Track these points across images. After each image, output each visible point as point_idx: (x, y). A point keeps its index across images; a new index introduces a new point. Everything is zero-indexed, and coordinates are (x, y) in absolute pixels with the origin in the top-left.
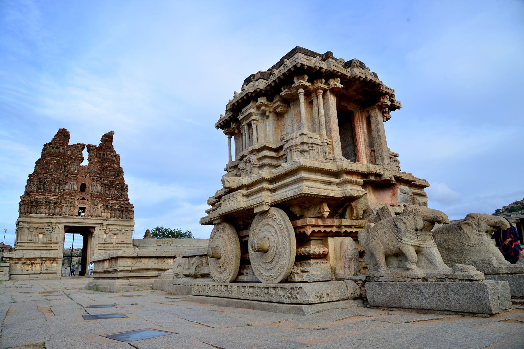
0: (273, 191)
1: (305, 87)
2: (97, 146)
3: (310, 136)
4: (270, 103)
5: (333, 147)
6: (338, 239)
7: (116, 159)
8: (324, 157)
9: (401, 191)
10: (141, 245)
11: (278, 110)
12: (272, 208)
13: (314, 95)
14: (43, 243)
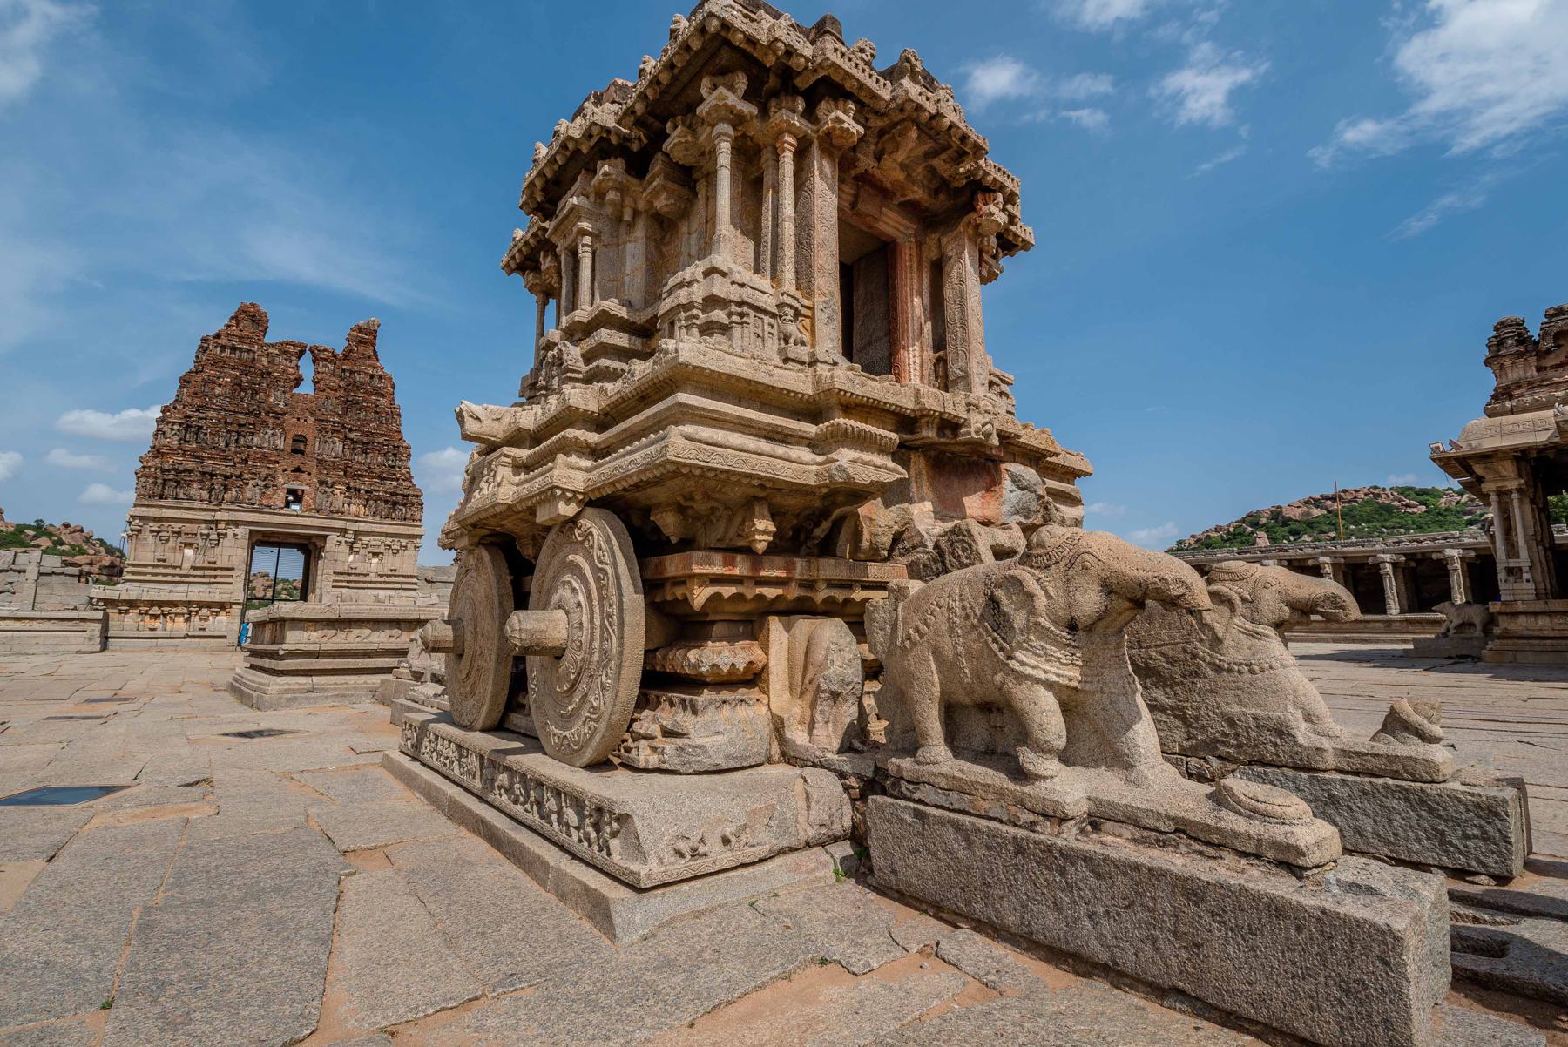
1: (738, 120)
2: (339, 351)
3: (737, 277)
4: (633, 180)
5: (813, 326)
6: (804, 625)
7: (381, 387)
8: (781, 351)
9: (1015, 479)
10: (439, 578)
11: (661, 203)
12: (589, 511)
13: (767, 155)
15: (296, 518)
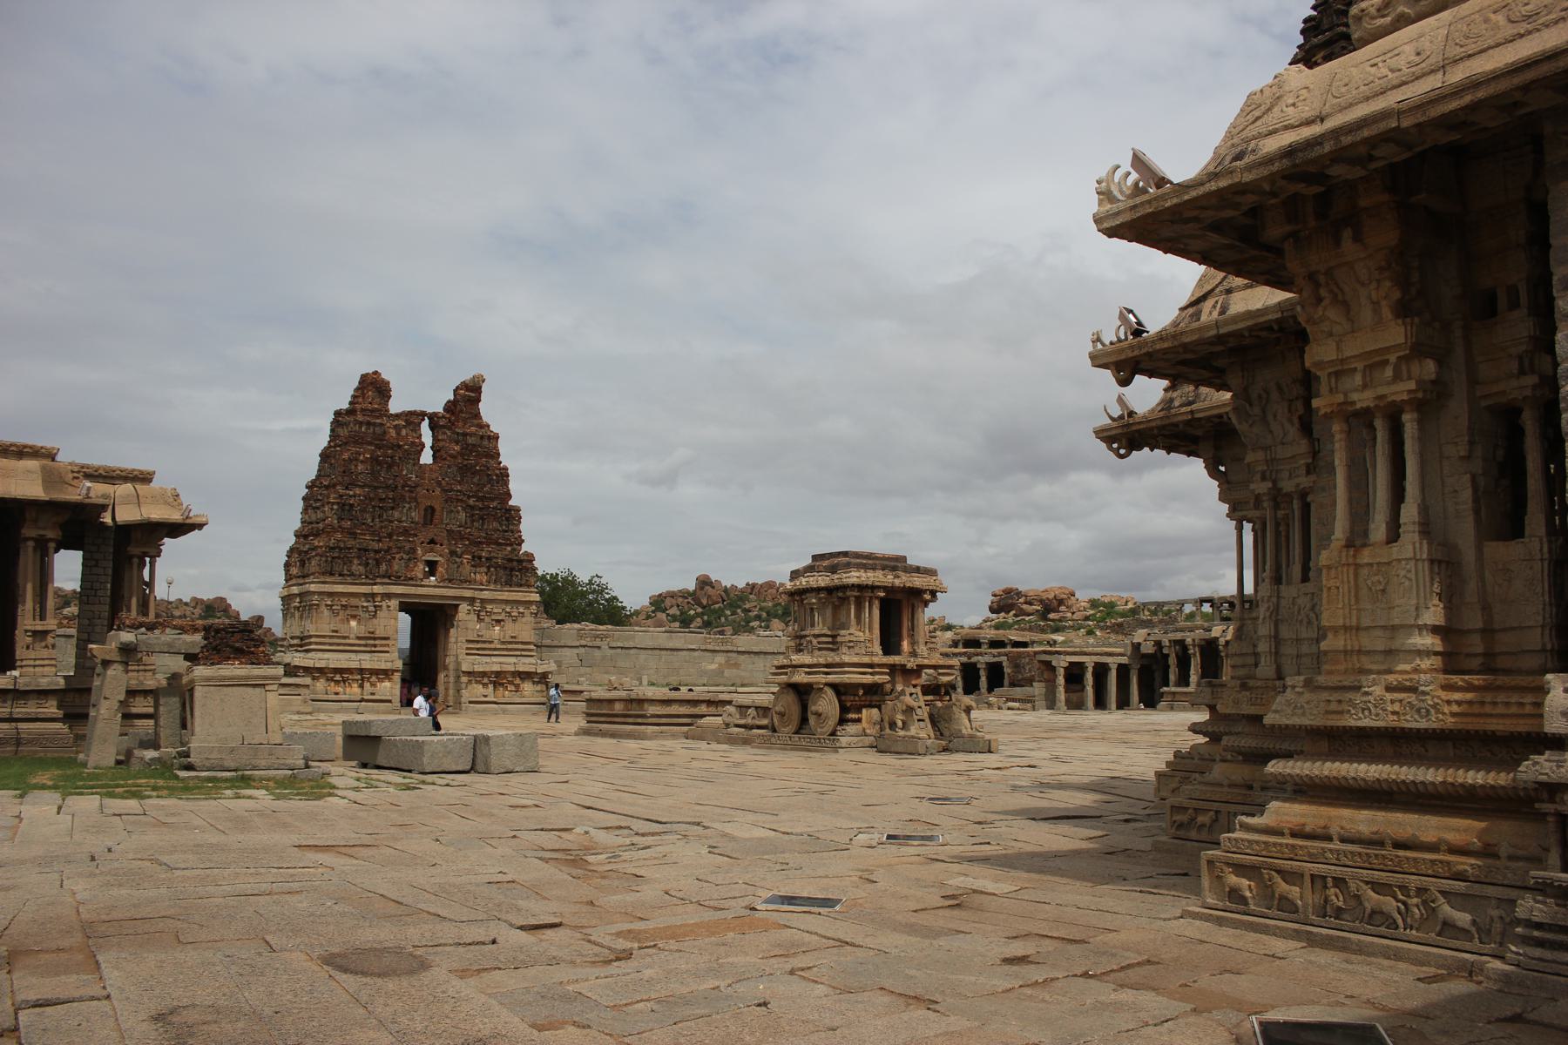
7: (487, 444)
14: (359, 638)
15: (431, 589)
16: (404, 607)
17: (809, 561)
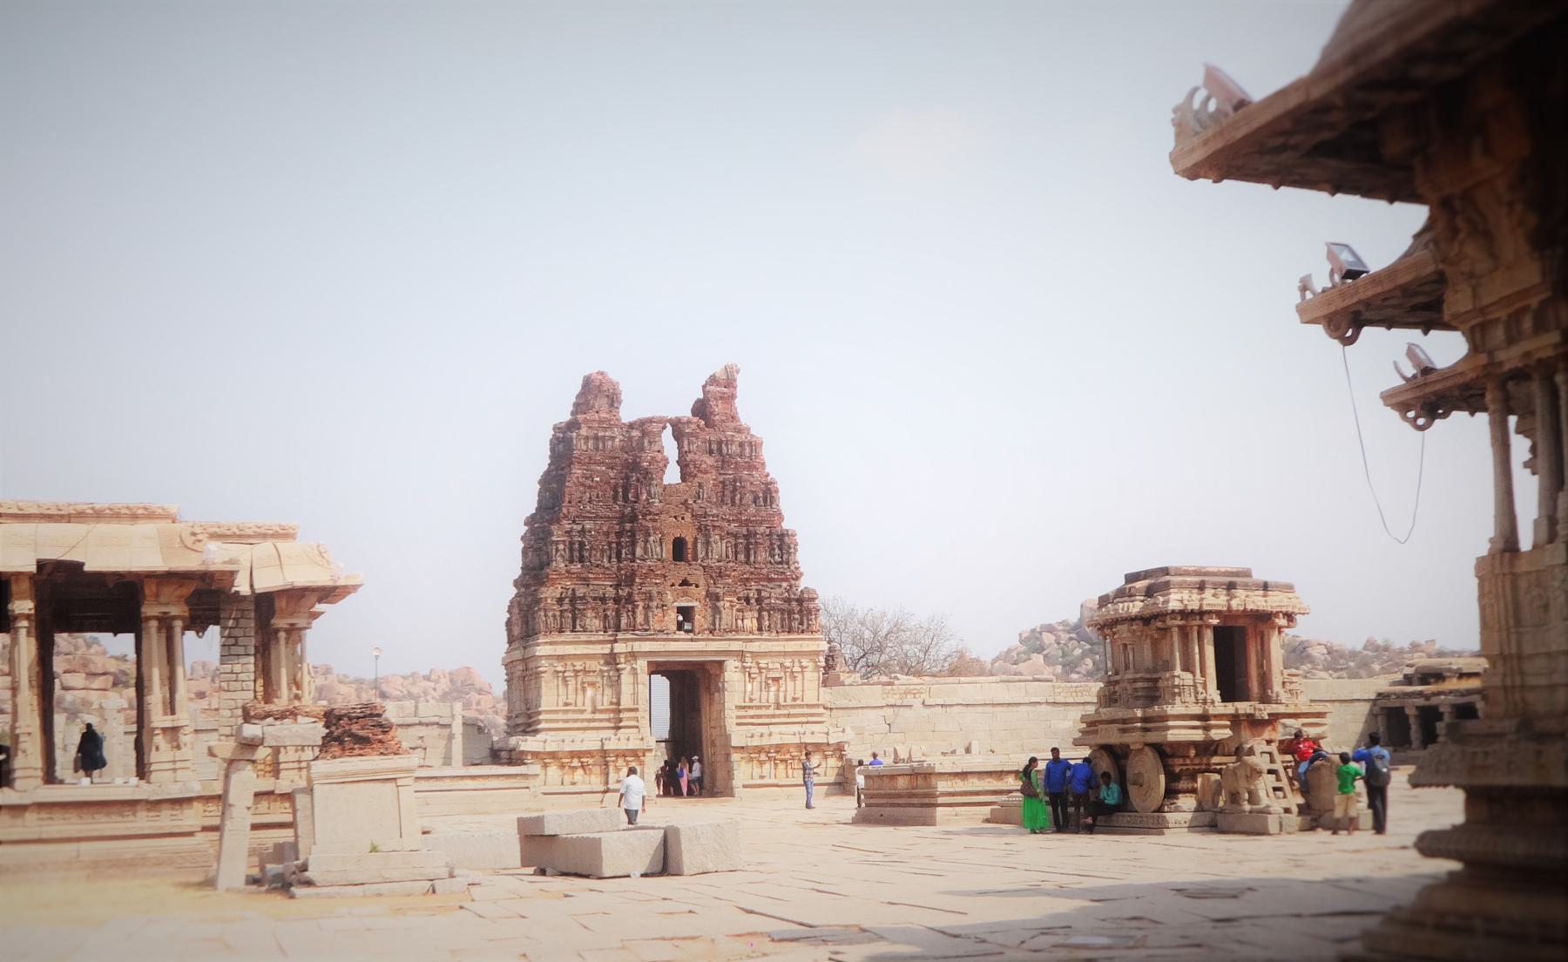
0: (1146, 730)
1: (1180, 627)
16: (656, 669)
17: (1121, 582)
